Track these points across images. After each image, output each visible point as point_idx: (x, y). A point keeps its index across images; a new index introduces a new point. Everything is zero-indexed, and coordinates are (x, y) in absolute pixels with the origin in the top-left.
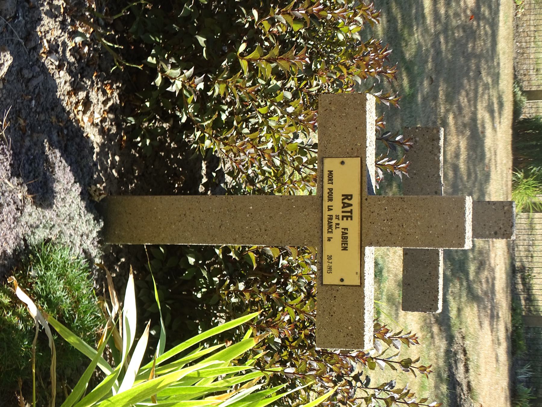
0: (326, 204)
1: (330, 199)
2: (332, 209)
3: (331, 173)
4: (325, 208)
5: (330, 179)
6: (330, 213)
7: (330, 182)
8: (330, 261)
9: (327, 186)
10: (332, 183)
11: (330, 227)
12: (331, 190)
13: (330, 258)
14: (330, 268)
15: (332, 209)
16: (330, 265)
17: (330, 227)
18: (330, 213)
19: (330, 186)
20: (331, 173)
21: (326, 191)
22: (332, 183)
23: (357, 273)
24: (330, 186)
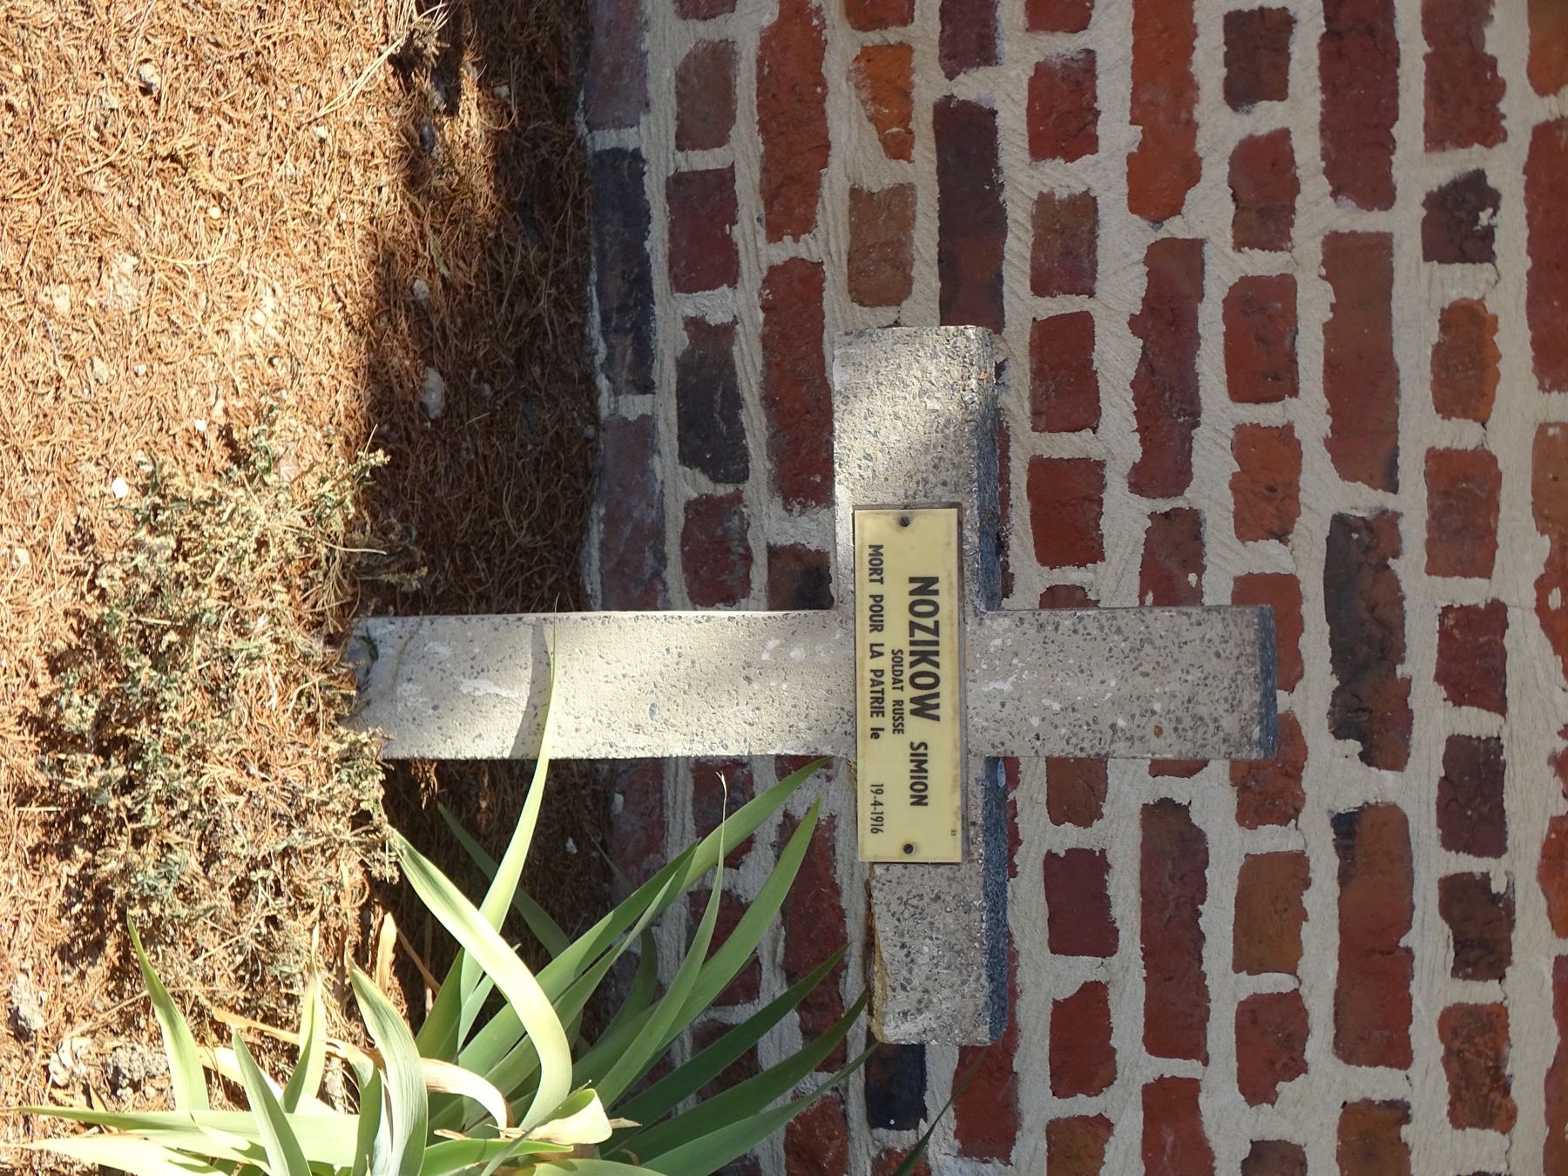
0: (866, 637)
1: (877, 626)
2: (881, 654)
3: (877, 550)
4: (863, 652)
5: (876, 570)
6: (878, 663)
7: (875, 577)
8: (880, 798)
9: (866, 589)
10: (881, 581)
11: (878, 700)
12: (878, 599)
13: (878, 790)
14: (879, 819)
15: (881, 654)
16: (879, 809)
17: (878, 700)
18: (878, 663)
19: (876, 589)
20: (877, 550)
21: (864, 604)
22: (881, 581)
23: (953, 833)
24: (876, 589)
